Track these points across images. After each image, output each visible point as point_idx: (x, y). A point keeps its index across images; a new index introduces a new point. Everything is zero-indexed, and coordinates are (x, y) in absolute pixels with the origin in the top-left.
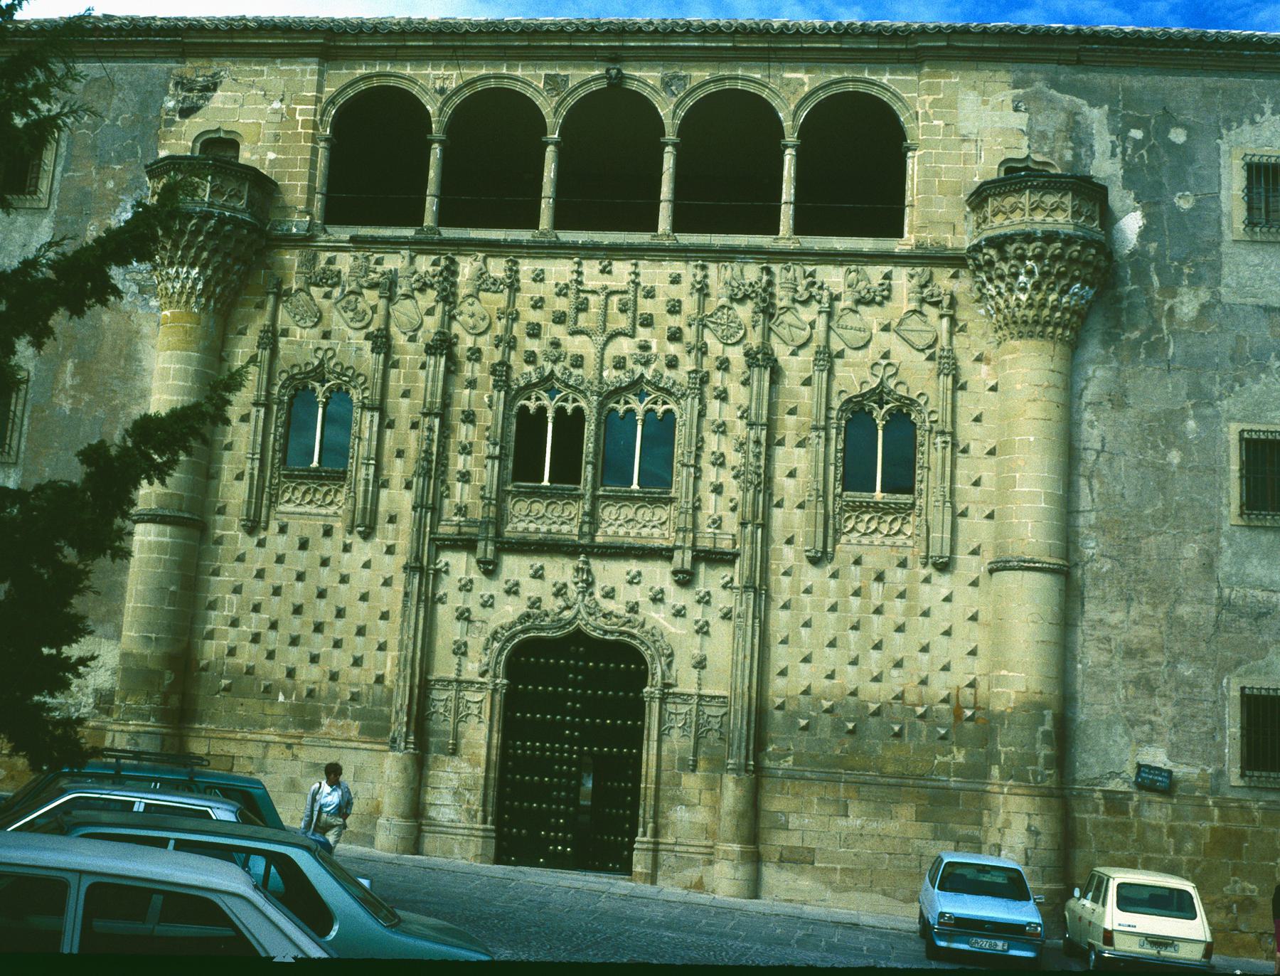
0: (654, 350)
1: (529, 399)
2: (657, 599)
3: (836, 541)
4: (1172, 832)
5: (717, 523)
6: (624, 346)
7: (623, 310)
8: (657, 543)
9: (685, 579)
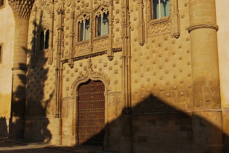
9: (111, 58)
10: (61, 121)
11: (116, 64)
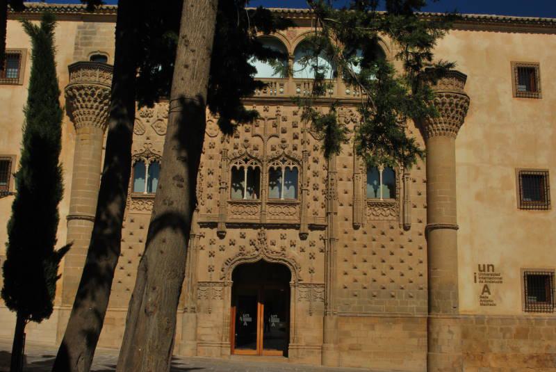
0: (288, 142)
1: (236, 163)
2: (293, 245)
4: (502, 329)
5: (316, 213)
6: (274, 141)
7: (275, 126)
8: (293, 222)
10: (197, 318)
11: (312, 245)
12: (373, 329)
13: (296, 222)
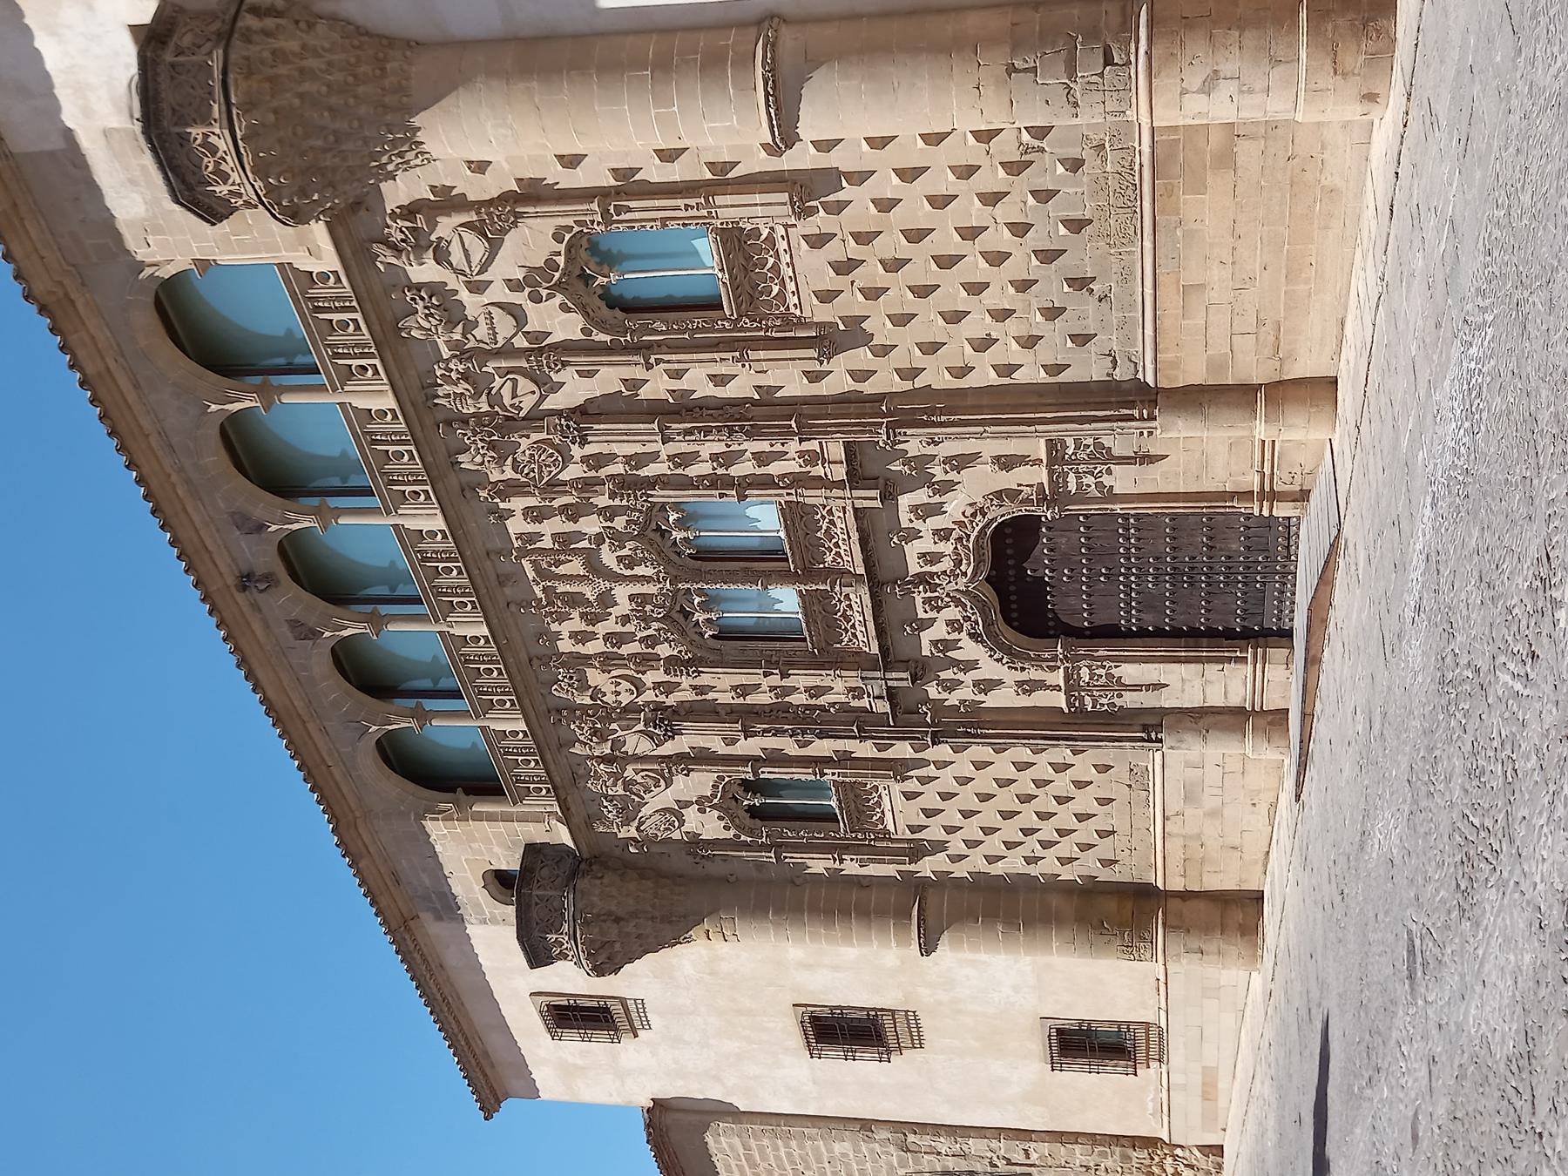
3: (802, 323)
5: (812, 458)
7: (558, 563)
12: (1202, 286)
13: (849, 508)
